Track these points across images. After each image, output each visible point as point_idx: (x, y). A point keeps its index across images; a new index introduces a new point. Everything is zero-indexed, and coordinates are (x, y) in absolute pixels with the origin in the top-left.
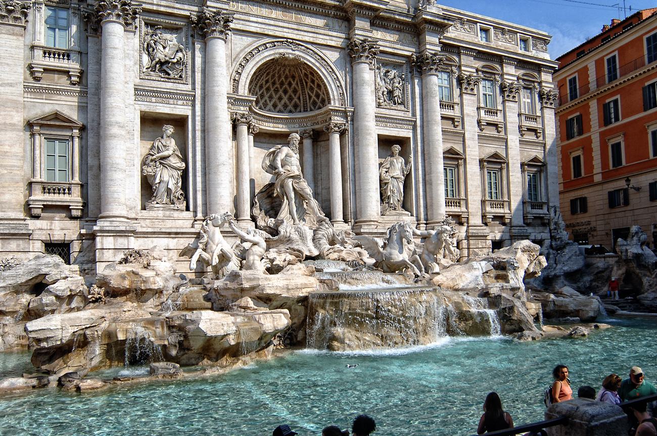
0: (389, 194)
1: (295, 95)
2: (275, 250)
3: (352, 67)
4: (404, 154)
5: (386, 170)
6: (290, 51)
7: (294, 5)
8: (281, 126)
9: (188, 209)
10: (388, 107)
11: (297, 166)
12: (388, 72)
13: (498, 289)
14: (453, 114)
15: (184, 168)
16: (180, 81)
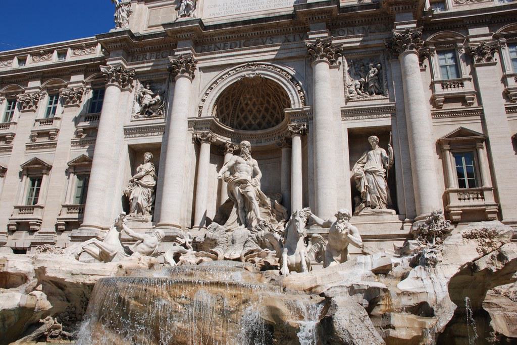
0: (363, 190)
1: (275, 111)
2: (195, 252)
3: (312, 68)
4: (383, 144)
5: (362, 165)
6: (250, 72)
7: (253, 35)
8: (263, 140)
9: (152, 221)
10: (362, 99)
11: (247, 172)
12: (363, 65)
13: (345, 290)
14: (463, 91)
15: (153, 185)
16: (159, 117)
